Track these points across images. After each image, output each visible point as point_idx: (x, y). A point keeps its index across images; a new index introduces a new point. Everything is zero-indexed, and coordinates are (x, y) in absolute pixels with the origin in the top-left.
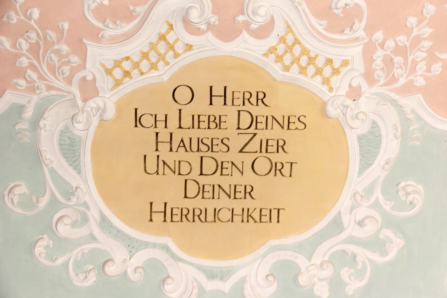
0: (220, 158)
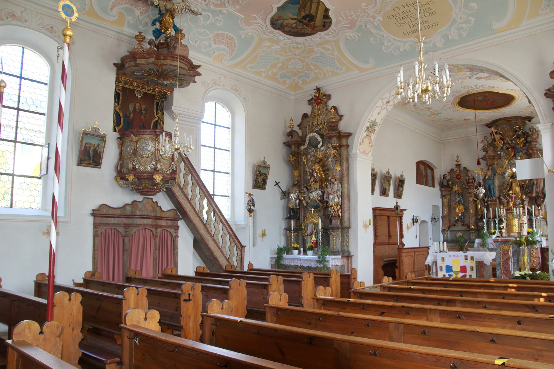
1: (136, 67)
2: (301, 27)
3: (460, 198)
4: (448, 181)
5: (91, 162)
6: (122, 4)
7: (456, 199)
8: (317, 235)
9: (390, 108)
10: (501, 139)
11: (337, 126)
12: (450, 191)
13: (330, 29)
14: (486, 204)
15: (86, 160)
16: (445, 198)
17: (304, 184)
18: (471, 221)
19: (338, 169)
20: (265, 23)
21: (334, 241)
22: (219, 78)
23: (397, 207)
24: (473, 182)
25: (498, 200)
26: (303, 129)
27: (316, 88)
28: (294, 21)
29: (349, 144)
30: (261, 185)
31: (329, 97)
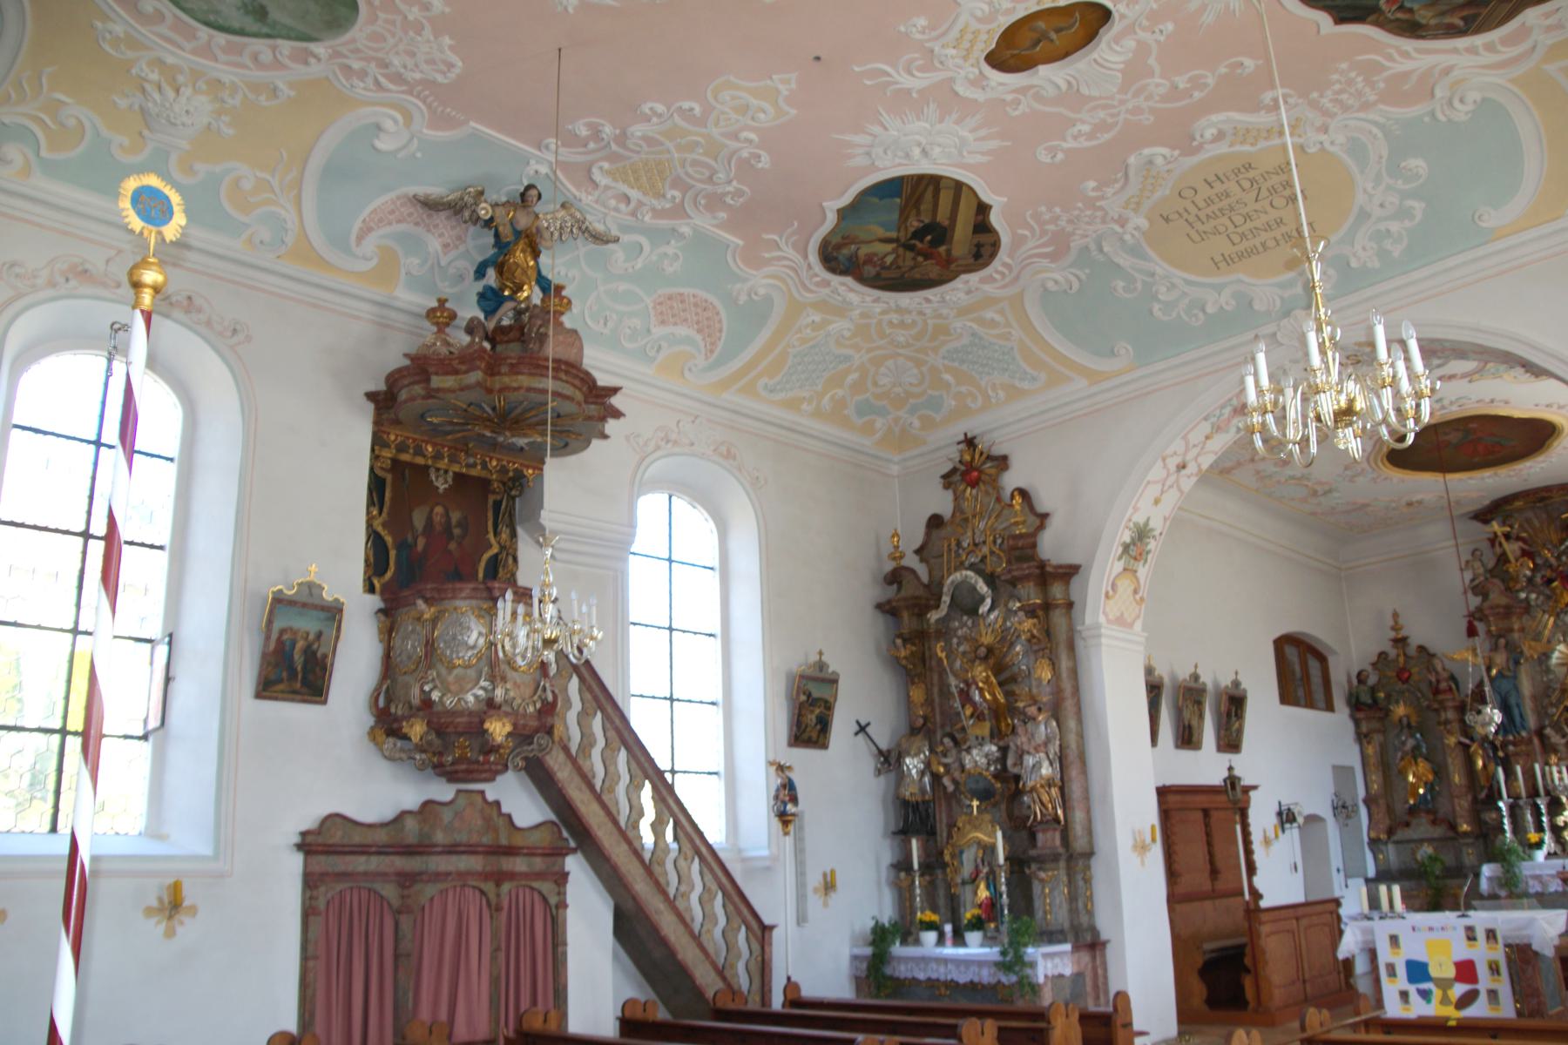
0: (1244, 211)
1: (430, 401)
2: (909, 263)
3: (1416, 739)
4: (1373, 690)
5: (298, 685)
6: (390, 224)
7: (1404, 743)
8: (992, 882)
9: (1188, 483)
10: (1524, 553)
11: (1034, 546)
12: (1381, 719)
13: (996, 264)
14: (1501, 754)
15: (280, 681)
16: (1369, 743)
17: (943, 726)
18: (1458, 808)
19: (1047, 675)
20: (806, 257)
21: (1045, 898)
22: (678, 422)
23: (1232, 781)
24: (1450, 689)
25: (1536, 741)
26: (932, 561)
27: (962, 437)
28: (889, 247)
29: (1074, 597)
30: (814, 735)
31: (1002, 462)
